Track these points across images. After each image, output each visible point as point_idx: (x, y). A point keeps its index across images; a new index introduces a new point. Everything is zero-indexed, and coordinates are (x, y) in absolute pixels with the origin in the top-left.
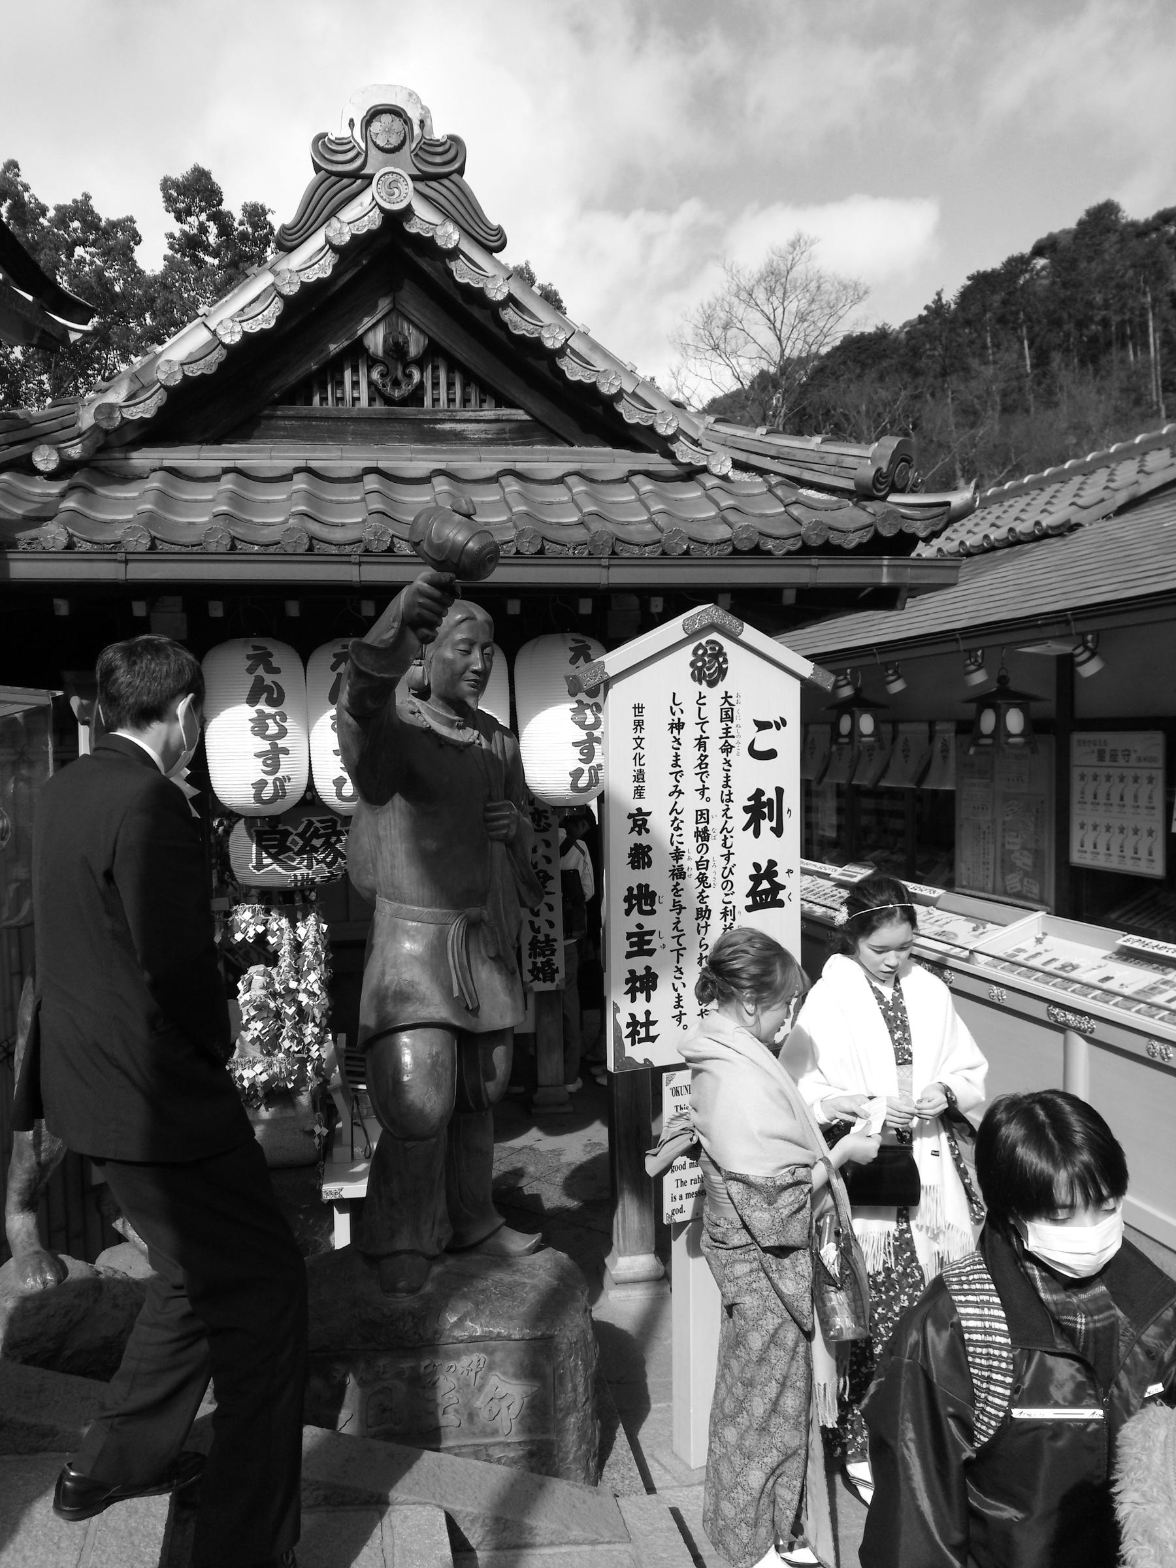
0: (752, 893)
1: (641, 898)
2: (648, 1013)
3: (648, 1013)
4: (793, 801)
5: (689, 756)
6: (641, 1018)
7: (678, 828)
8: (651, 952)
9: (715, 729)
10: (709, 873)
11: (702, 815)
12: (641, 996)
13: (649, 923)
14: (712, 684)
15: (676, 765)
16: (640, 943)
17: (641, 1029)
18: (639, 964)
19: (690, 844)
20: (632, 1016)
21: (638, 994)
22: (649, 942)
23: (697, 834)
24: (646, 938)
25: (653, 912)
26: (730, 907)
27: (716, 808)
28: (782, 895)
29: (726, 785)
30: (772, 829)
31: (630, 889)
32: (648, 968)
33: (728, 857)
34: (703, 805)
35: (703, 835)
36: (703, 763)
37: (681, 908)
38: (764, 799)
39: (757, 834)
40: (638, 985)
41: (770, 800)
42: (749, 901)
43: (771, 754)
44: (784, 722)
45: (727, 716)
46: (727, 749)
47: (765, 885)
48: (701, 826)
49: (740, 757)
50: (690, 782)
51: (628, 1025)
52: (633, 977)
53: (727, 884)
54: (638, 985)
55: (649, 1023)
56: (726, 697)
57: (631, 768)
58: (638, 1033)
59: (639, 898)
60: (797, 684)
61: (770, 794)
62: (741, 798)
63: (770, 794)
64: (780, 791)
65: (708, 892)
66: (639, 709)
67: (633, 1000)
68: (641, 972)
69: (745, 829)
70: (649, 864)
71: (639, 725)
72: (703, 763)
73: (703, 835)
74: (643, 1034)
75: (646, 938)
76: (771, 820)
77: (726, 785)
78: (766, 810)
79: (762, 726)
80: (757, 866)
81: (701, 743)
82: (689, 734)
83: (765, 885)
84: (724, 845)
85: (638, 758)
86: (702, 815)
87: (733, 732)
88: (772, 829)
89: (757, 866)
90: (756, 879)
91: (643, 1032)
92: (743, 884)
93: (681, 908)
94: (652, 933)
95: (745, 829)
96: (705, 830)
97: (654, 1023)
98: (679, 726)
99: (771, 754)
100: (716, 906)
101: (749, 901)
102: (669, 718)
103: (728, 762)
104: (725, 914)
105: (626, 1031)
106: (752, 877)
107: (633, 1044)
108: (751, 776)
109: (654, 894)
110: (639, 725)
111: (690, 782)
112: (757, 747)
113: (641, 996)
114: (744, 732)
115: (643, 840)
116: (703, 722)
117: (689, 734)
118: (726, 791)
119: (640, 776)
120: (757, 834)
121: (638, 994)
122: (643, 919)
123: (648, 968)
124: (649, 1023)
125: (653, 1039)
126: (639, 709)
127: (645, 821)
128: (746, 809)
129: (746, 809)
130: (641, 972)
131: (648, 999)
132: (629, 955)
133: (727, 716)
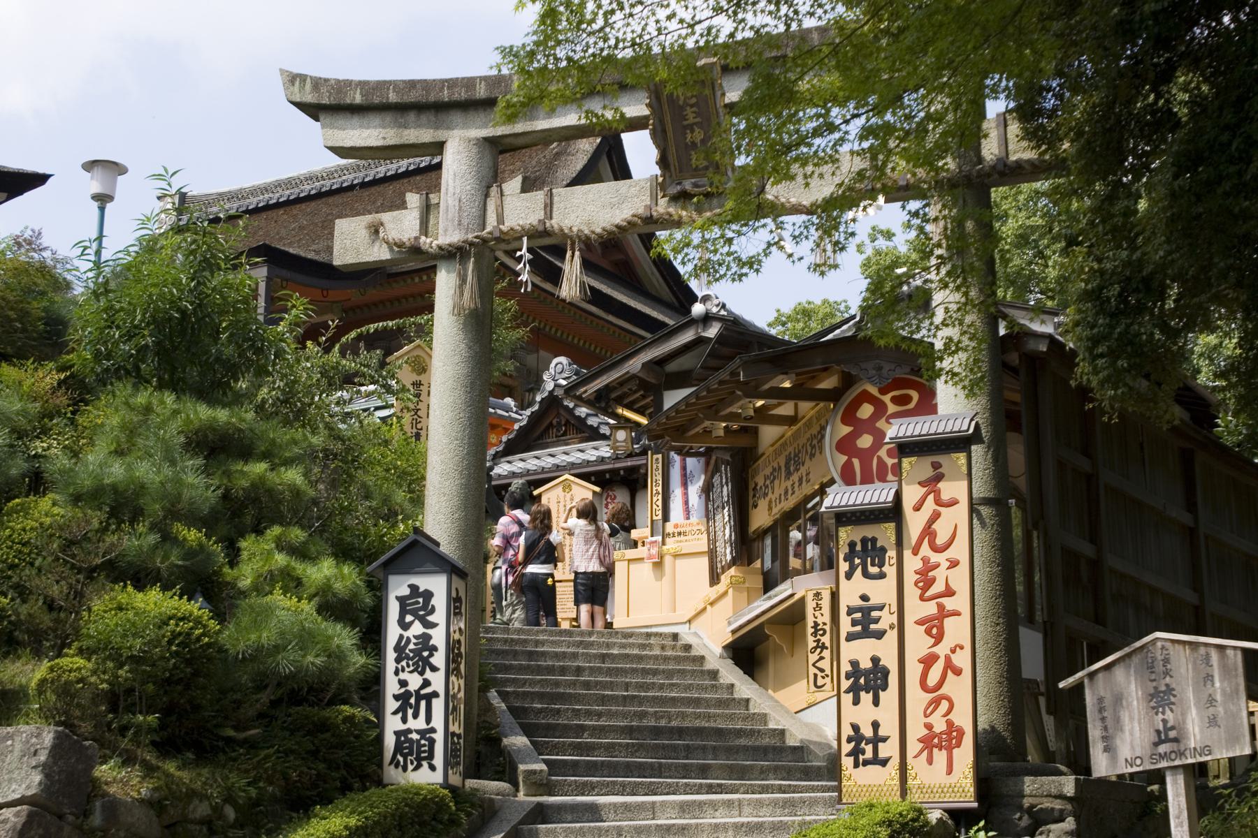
2: (876, 725)
3: (876, 725)
6: (867, 732)
12: (866, 698)
20: (856, 728)
21: (863, 694)
22: (877, 621)
24: (875, 614)
25: (882, 576)
32: (875, 660)
40: (862, 681)
51: (849, 740)
54: (862, 681)
55: (877, 740)
58: (863, 752)
67: (856, 702)
68: (866, 664)
74: (869, 754)
75: (875, 614)
91: (869, 749)
94: (881, 608)
97: (884, 740)
105: (847, 748)
107: (856, 765)
113: (866, 698)
121: (863, 694)
123: (875, 660)
124: (877, 740)
125: (884, 763)
130: (866, 664)
131: (876, 702)
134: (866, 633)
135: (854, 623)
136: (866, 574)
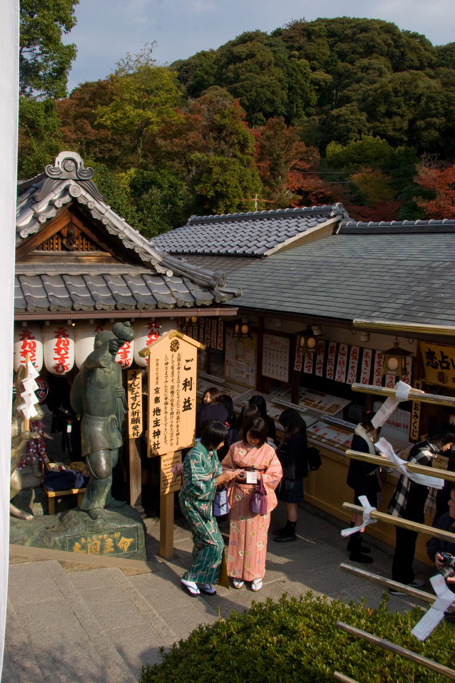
0: (184, 407)
4: (194, 381)
5: (170, 371)
6: (156, 443)
8: (159, 425)
9: (176, 363)
11: (172, 387)
12: (156, 437)
13: (159, 417)
14: (175, 351)
16: (157, 423)
17: (157, 445)
18: (156, 429)
19: (169, 395)
23: (171, 392)
34: (172, 384)
35: (172, 392)
36: (173, 373)
39: (185, 390)
42: (183, 409)
43: (189, 369)
45: (179, 360)
46: (179, 368)
47: (187, 404)
49: (182, 370)
50: (170, 379)
52: (155, 432)
55: (158, 444)
56: (179, 355)
57: (155, 376)
59: (156, 411)
61: (189, 379)
62: (182, 382)
64: (191, 378)
66: (157, 360)
68: (156, 431)
71: (157, 364)
72: (173, 373)
73: (172, 392)
79: (187, 361)
80: (185, 399)
81: (172, 368)
82: (169, 366)
83: (187, 404)
85: (157, 374)
86: (172, 387)
89: (185, 399)
90: (185, 403)
91: (157, 446)
98: (167, 364)
99: (189, 369)
100: (175, 411)
102: (165, 362)
110: (157, 364)
111: (170, 379)
114: (183, 363)
115: (158, 395)
116: (173, 362)
117: (169, 366)
119: (157, 378)
120: (185, 390)
128: (183, 384)
129: (183, 384)
132: (154, 427)
133: (179, 360)
136: (157, 415)
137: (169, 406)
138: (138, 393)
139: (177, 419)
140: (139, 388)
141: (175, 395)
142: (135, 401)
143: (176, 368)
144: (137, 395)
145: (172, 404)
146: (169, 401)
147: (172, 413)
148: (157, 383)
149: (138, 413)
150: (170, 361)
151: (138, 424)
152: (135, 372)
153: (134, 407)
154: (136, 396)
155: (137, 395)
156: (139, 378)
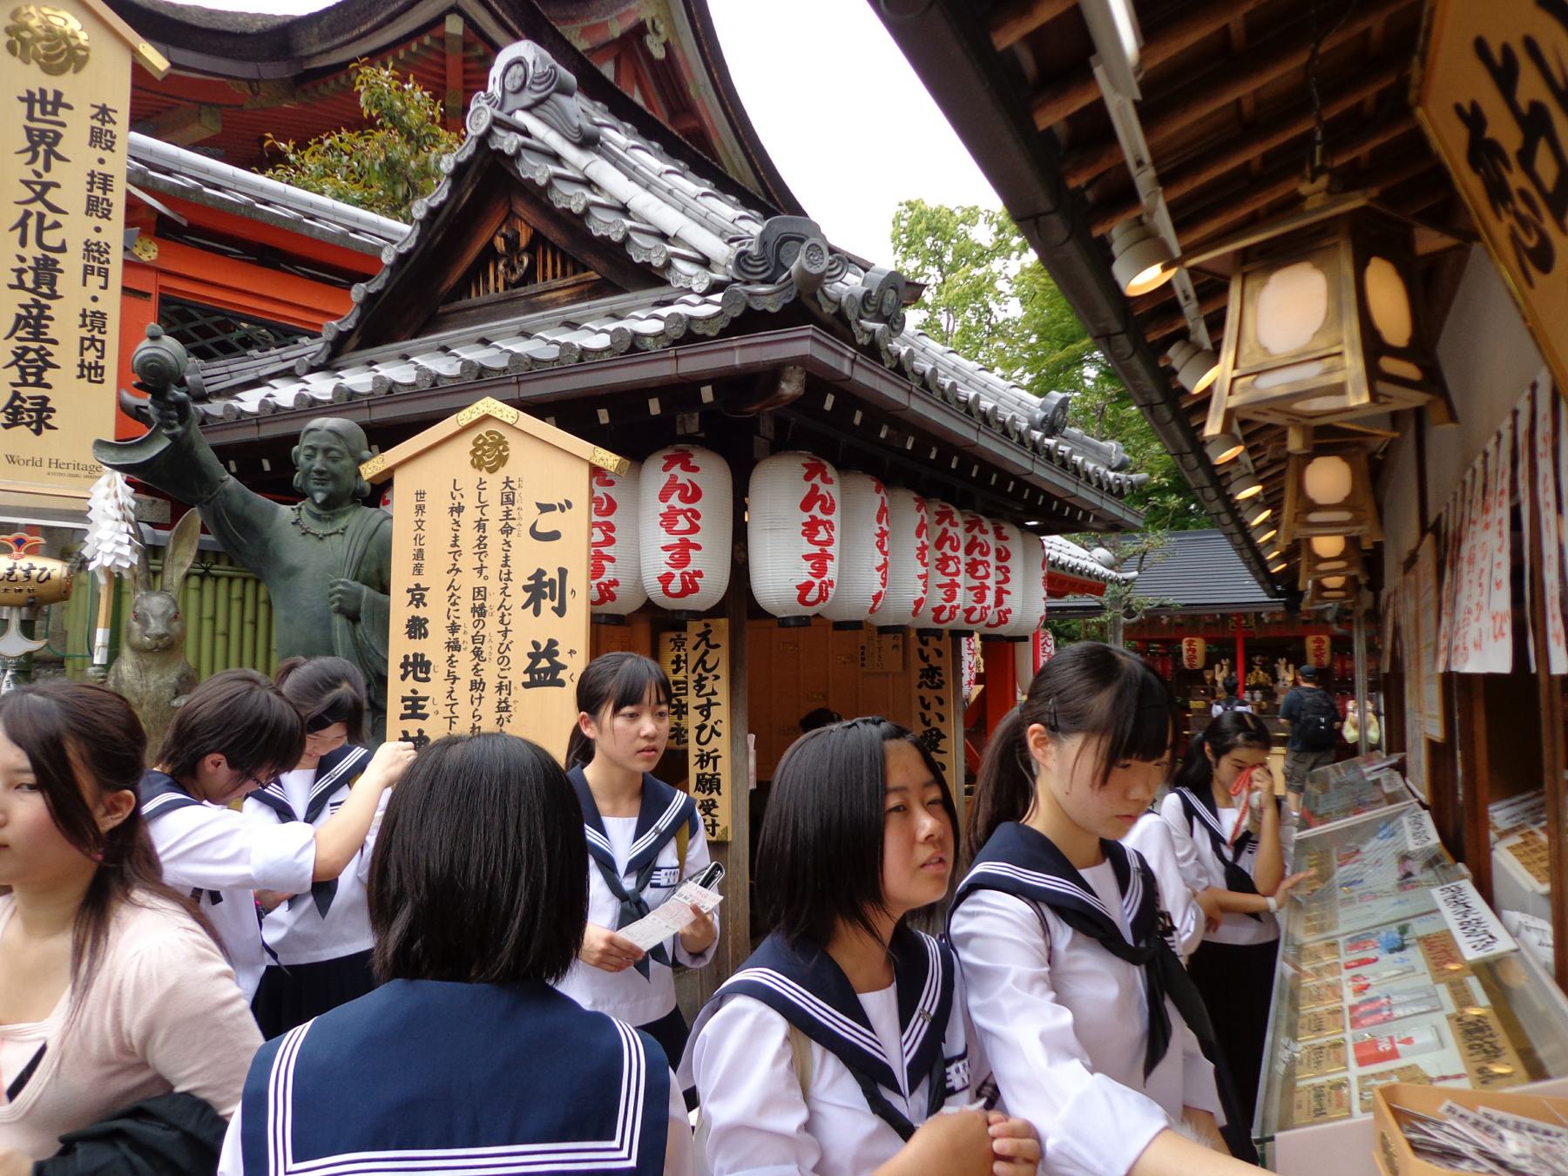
0: (530, 670)
1: (417, 666)
5: (469, 537)
7: (454, 604)
9: (495, 513)
10: (484, 648)
11: (480, 592)
14: (492, 471)
15: (455, 545)
19: (466, 619)
22: (422, 707)
23: (474, 610)
25: (427, 680)
26: (505, 682)
27: (494, 586)
28: (562, 675)
29: (505, 565)
30: (553, 609)
31: (406, 657)
32: (420, 732)
33: (505, 633)
34: (481, 583)
35: (480, 611)
36: (481, 543)
37: (455, 678)
38: (545, 579)
39: (537, 612)
41: (552, 581)
42: (527, 678)
43: (554, 536)
44: (569, 505)
45: (508, 500)
46: (507, 530)
47: (544, 663)
48: (478, 603)
50: (468, 561)
53: (503, 659)
56: (508, 482)
60: (585, 471)
61: (552, 574)
62: (521, 577)
63: (552, 574)
64: (563, 572)
65: (482, 666)
66: (421, 494)
69: (524, 607)
70: (426, 635)
71: (420, 509)
72: (481, 543)
73: (480, 611)
76: (552, 599)
77: (505, 565)
78: (547, 590)
79: (545, 508)
80: (536, 644)
81: (481, 525)
82: (469, 517)
83: (544, 663)
84: (502, 622)
86: (480, 592)
87: (514, 514)
88: (553, 609)
89: (536, 644)
90: (535, 657)
92: (520, 661)
93: (455, 678)
94: (425, 699)
95: (524, 607)
96: (482, 606)
98: (459, 509)
99: (554, 536)
100: (491, 681)
101: (527, 678)
102: (450, 503)
103: (507, 543)
104: (500, 688)
106: (530, 655)
108: (529, 558)
109: (428, 664)
110: (420, 509)
111: (468, 561)
112: (538, 529)
114: (526, 514)
115: (421, 612)
117: (469, 517)
118: (505, 570)
119: (419, 555)
120: (537, 612)
122: (419, 686)
123: (420, 732)
126: (421, 494)
127: (423, 596)
128: (526, 589)
129: (526, 589)
132: (403, 717)
133: (508, 500)
134: (414, 716)
135: (406, 708)
136: (416, 678)
137: (465, 659)
138: (714, 693)
139: (500, 710)
140: (717, 678)
141: (492, 625)
142: (707, 717)
143: (493, 527)
144: (714, 699)
145: (477, 653)
146: (463, 637)
147: (477, 685)
148: (418, 570)
149: (715, 759)
150: (470, 502)
151: (714, 795)
152: (707, 625)
153: (703, 739)
154: (710, 704)
155: (714, 699)
156: (717, 646)
